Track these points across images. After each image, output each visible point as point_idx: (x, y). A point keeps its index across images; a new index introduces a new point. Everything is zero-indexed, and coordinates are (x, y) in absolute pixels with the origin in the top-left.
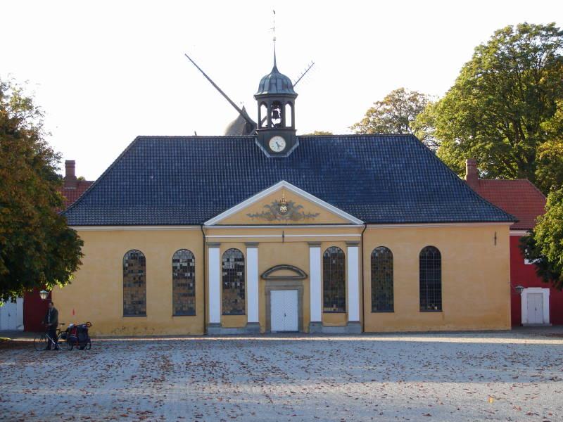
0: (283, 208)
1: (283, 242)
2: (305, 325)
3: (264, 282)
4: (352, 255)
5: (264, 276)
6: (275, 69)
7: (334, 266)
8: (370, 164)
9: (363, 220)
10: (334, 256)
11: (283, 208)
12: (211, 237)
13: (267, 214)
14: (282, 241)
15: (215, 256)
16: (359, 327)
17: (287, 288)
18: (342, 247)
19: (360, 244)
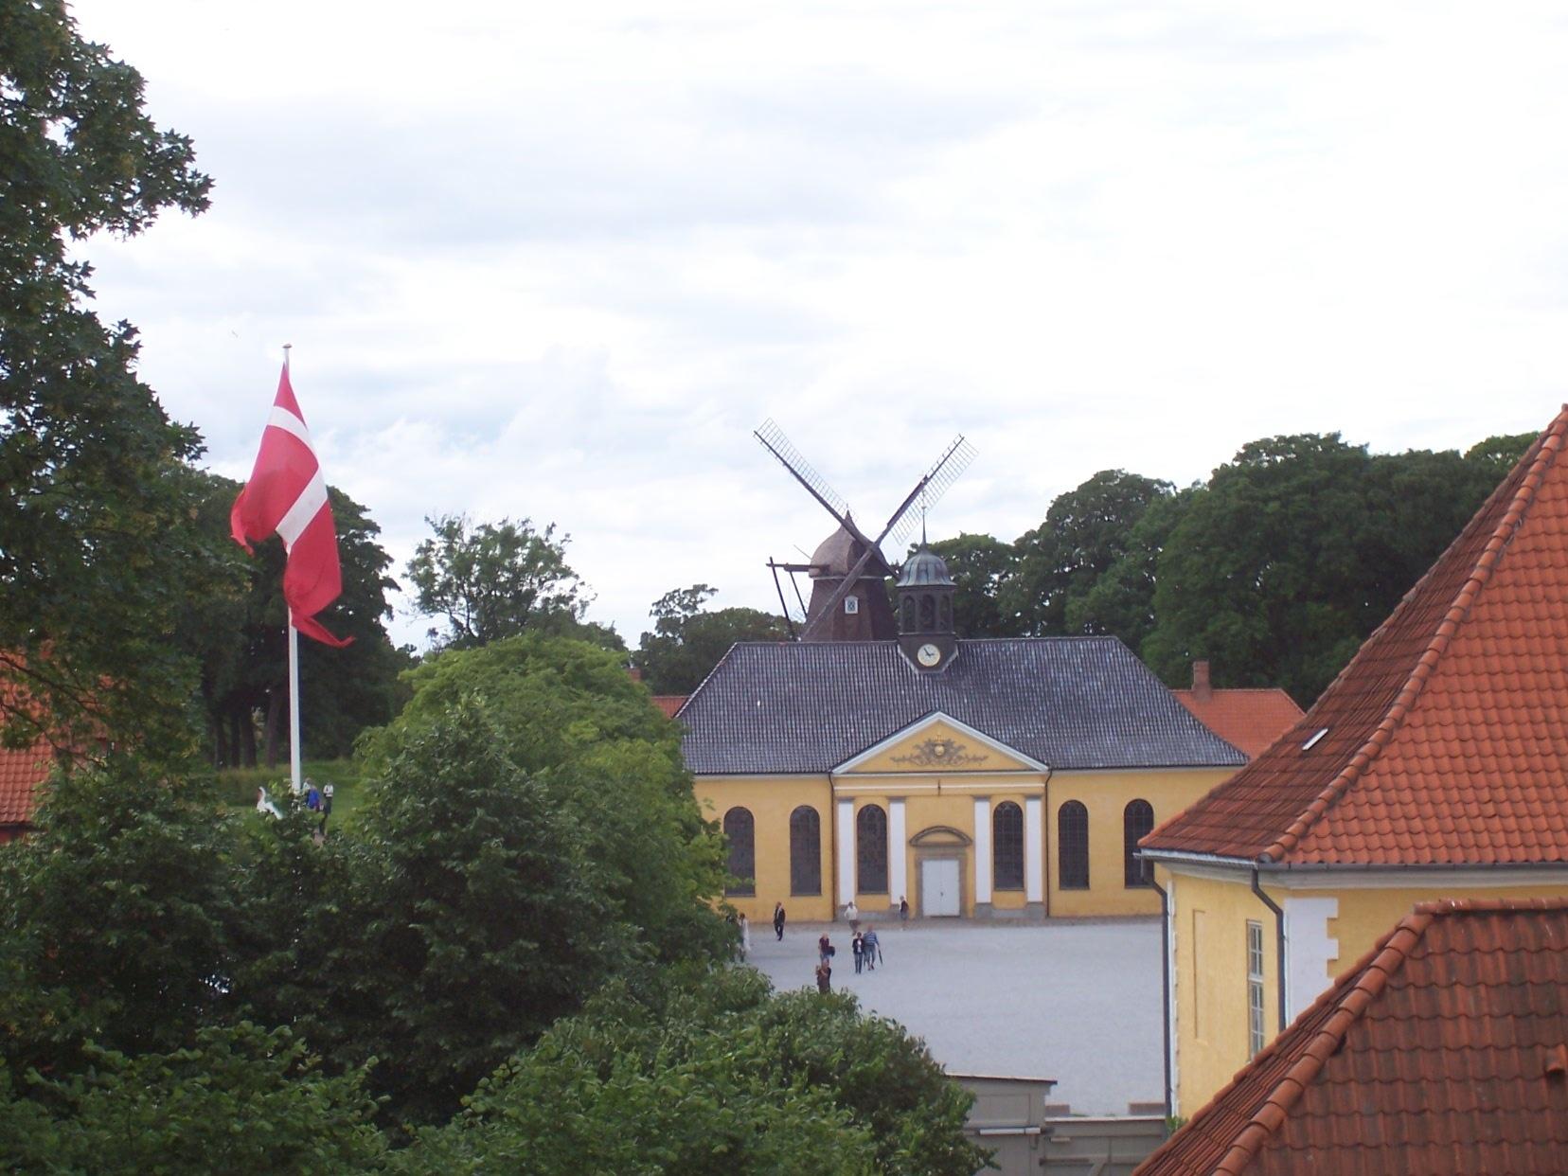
0: (940, 749)
1: (939, 795)
2: (970, 905)
3: (913, 851)
4: (1033, 813)
5: (915, 842)
7: (1008, 823)
8: (1056, 682)
9: (1047, 765)
10: (1008, 814)
11: (940, 749)
12: (842, 789)
13: (918, 757)
14: (936, 793)
15: (847, 817)
16: (1043, 909)
17: (944, 857)
18: (1018, 801)
19: (1044, 797)
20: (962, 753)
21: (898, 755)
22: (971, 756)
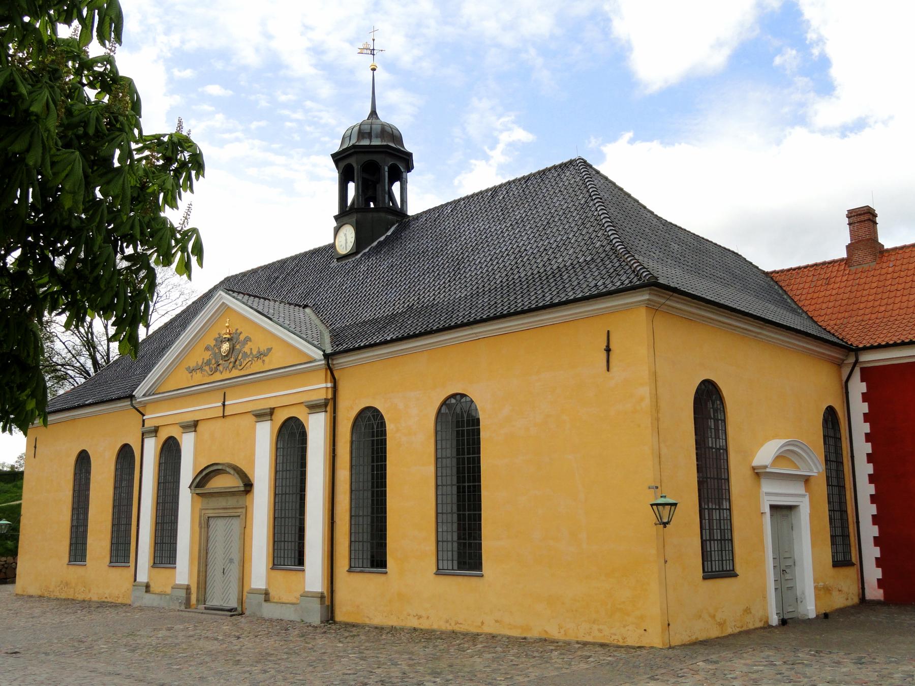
1: (224, 416)
6: (373, 113)
14: (222, 415)
19: (330, 405)
20: (246, 349)
21: (192, 364)
22: (255, 352)
